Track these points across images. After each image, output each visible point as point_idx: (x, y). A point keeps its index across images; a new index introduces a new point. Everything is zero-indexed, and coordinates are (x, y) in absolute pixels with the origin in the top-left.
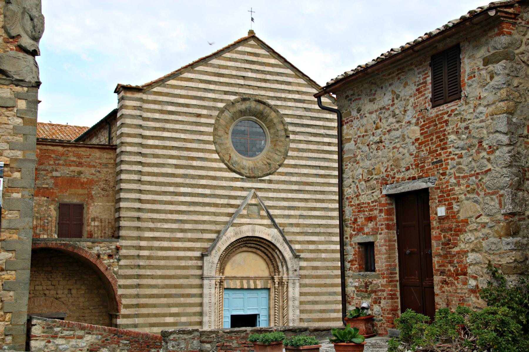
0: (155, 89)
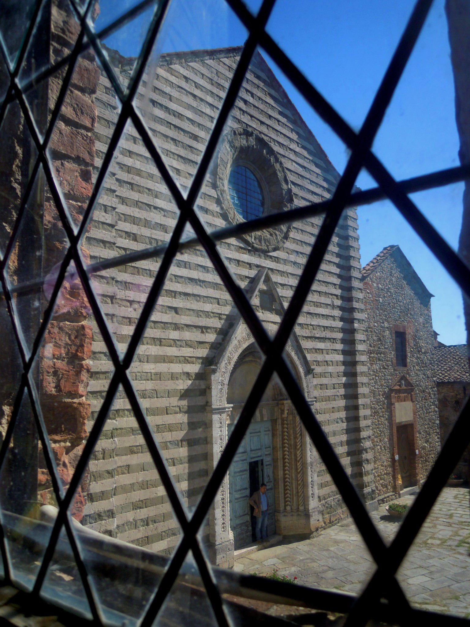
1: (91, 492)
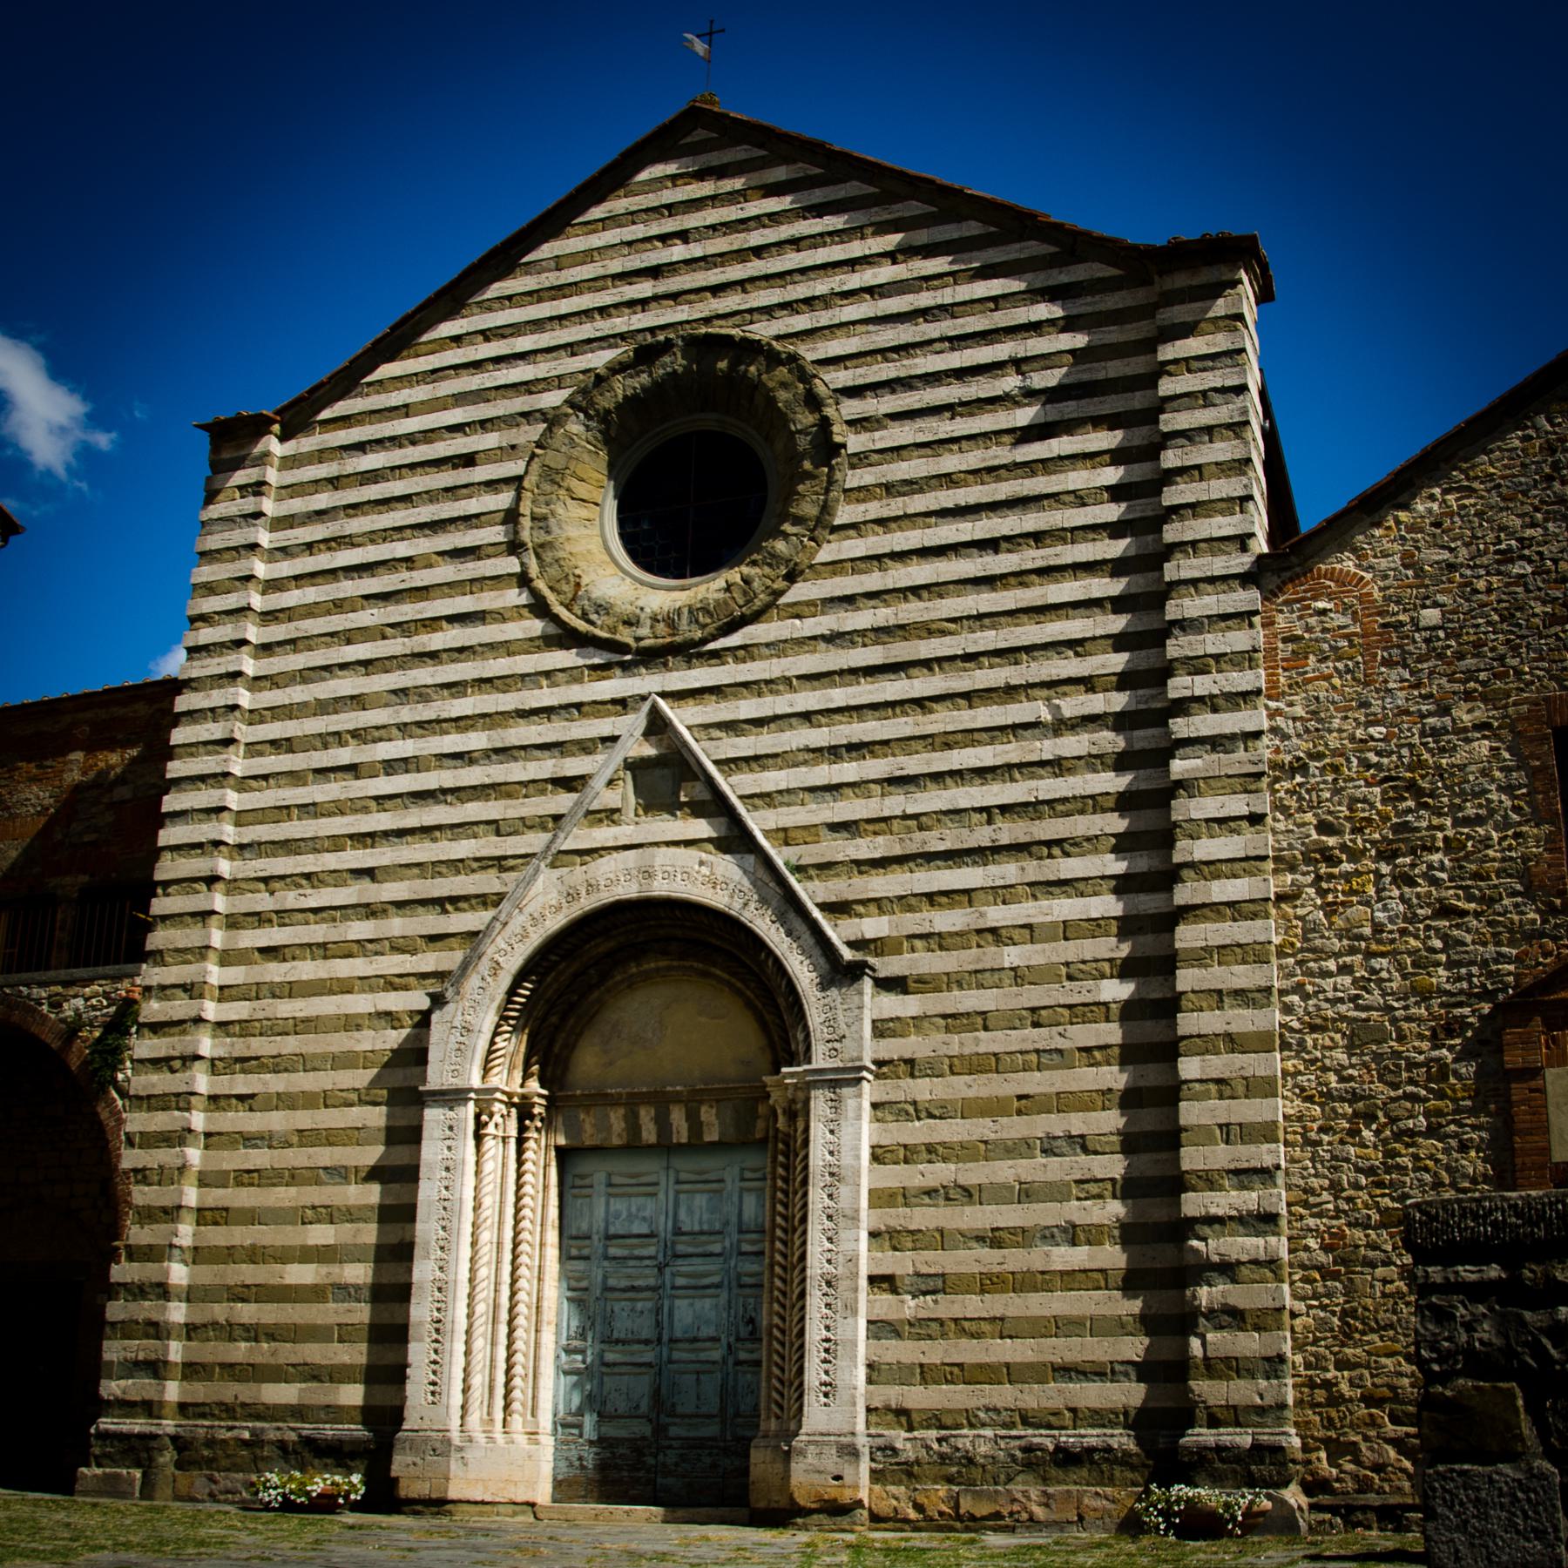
0: (325, 414)
1: (131, 1242)
